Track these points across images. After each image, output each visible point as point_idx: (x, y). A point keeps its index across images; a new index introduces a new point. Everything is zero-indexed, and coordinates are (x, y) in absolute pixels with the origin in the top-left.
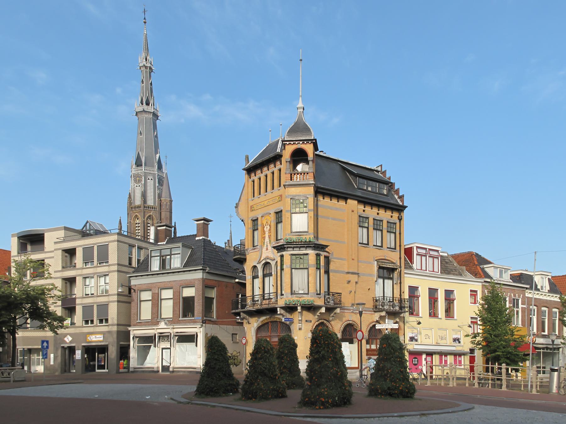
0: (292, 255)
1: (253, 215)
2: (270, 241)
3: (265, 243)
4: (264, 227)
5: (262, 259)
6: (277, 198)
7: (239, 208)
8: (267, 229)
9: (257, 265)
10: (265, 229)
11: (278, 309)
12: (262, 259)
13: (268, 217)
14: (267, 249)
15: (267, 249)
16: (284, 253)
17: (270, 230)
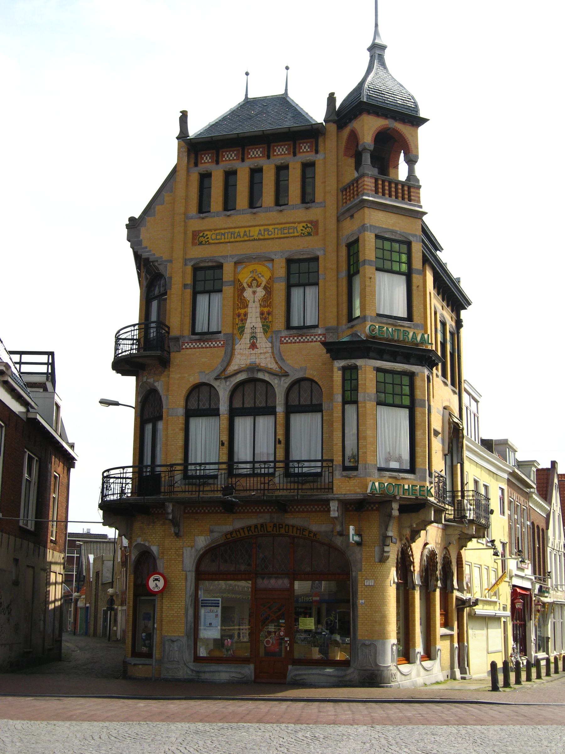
0: (378, 370)
1: (199, 253)
2: (266, 328)
3: (248, 330)
4: (243, 289)
5: (233, 367)
6: (300, 227)
7: (143, 230)
8: (254, 297)
9: (215, 384)
10: (248, 294)
11: (334, 506)
12: (233, 367)
13: (260, 268)
14: (253, 346)
15: (253, 346)
16: (359, 362)
17: (267, 301)
